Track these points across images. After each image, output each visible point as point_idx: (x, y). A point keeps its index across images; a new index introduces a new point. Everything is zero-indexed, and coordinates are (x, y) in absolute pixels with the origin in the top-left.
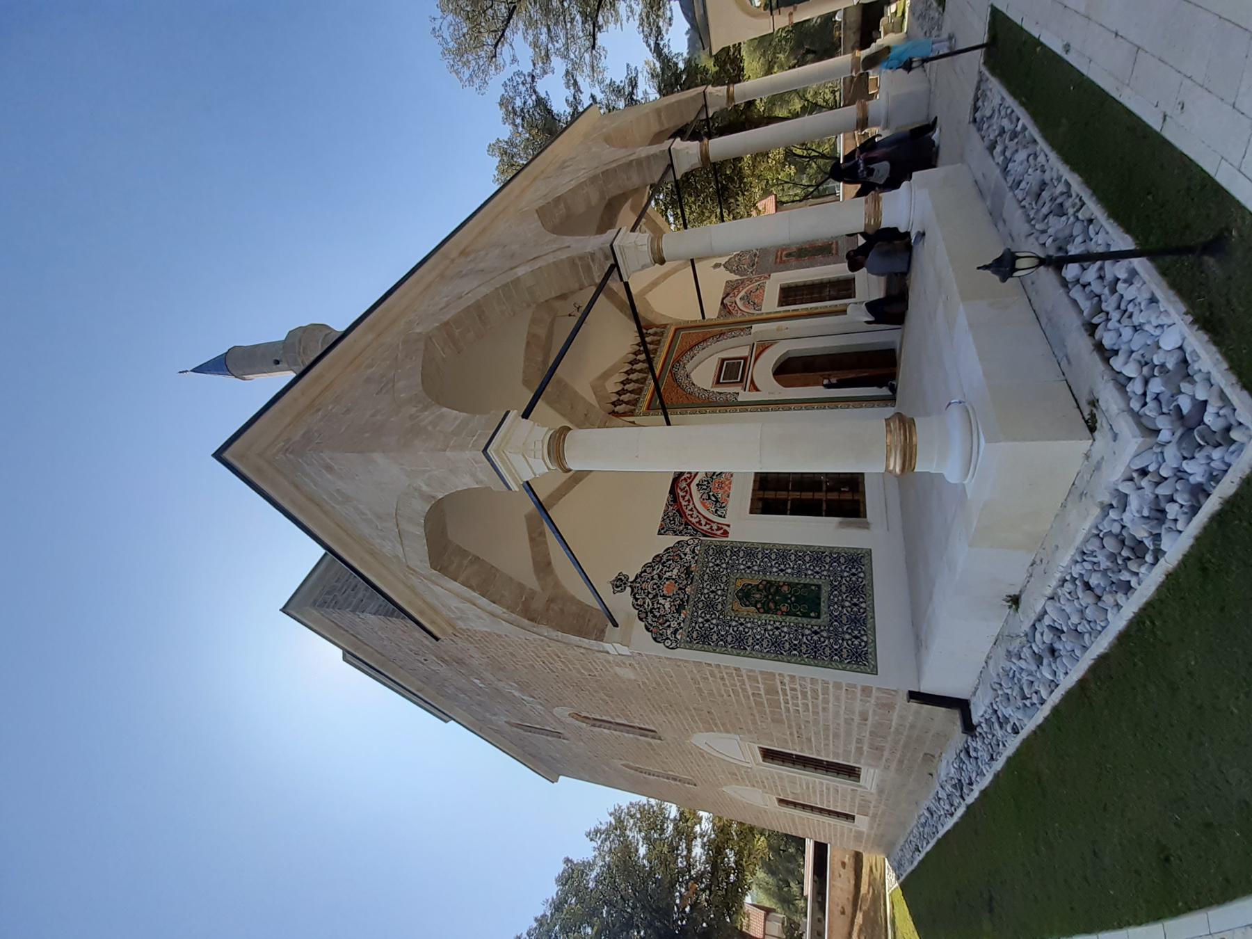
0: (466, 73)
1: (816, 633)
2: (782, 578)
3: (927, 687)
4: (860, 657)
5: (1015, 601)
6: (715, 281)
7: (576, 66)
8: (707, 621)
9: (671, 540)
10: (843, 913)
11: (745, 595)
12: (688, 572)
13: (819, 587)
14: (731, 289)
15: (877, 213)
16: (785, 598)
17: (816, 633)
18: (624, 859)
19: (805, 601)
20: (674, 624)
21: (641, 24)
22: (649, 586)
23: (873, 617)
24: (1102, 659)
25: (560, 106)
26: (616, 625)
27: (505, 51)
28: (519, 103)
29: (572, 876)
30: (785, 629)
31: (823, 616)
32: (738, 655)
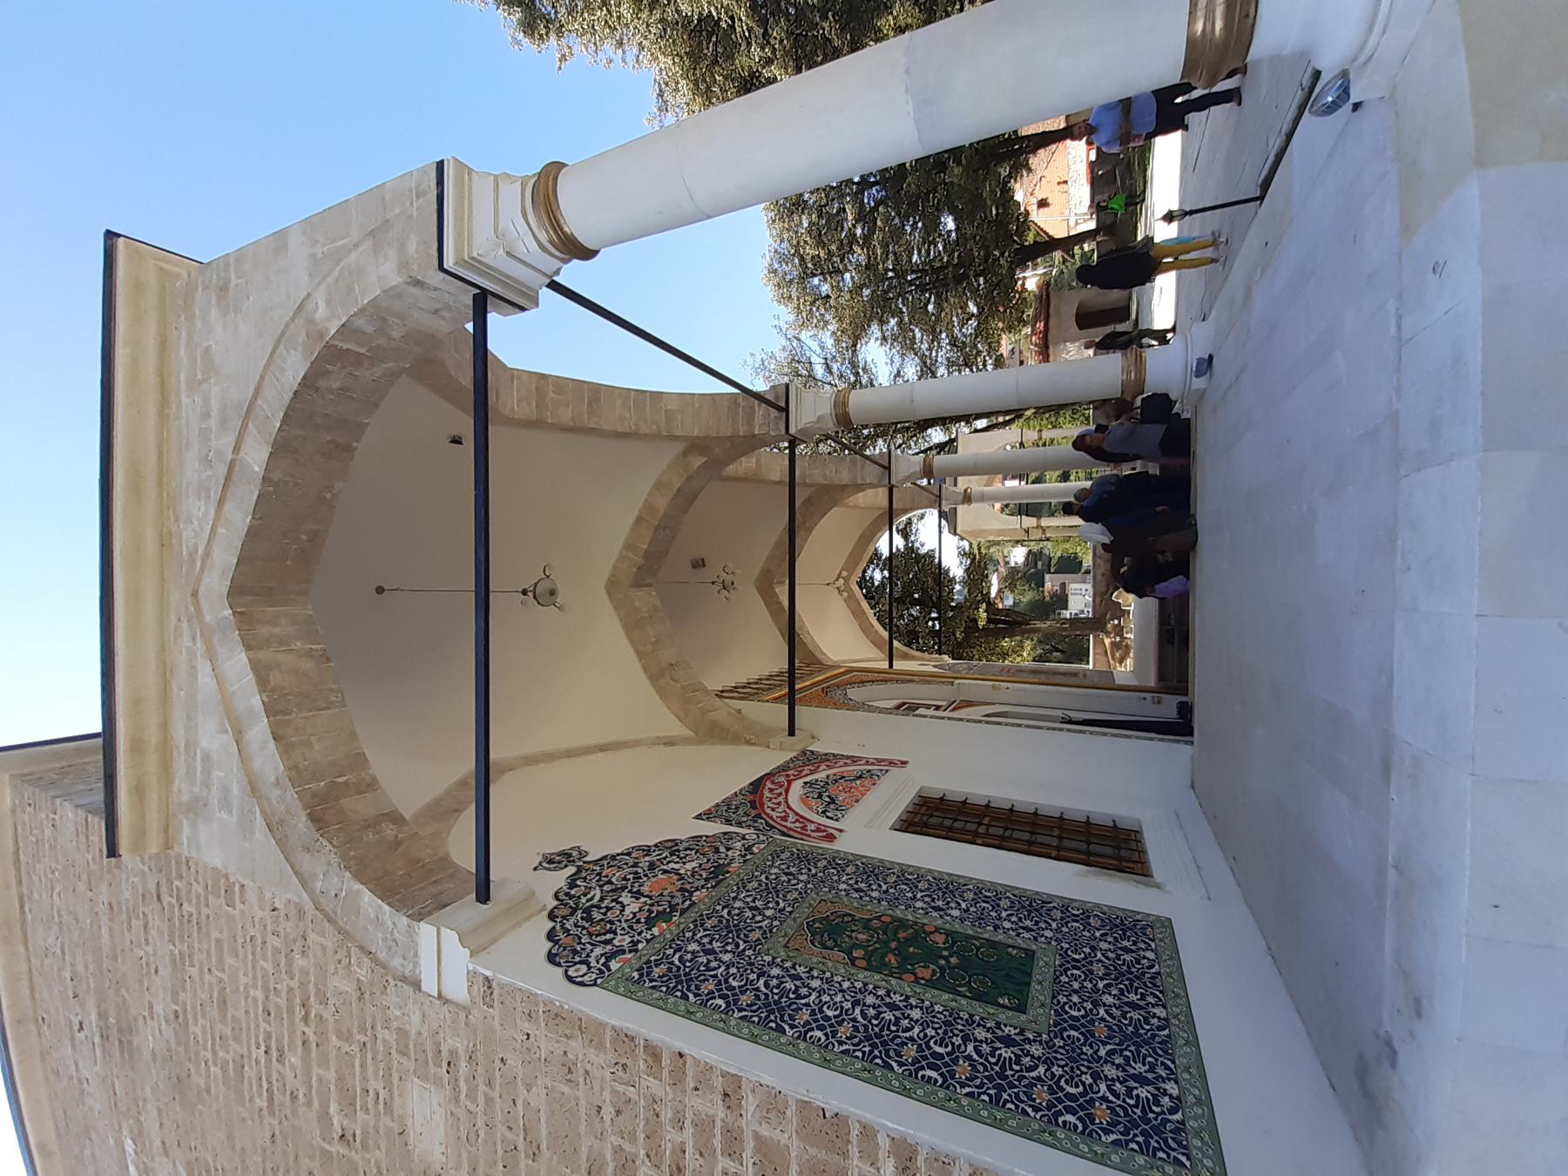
16: (932, 955)
31: (1039, 1015)
32: (753, 1039)
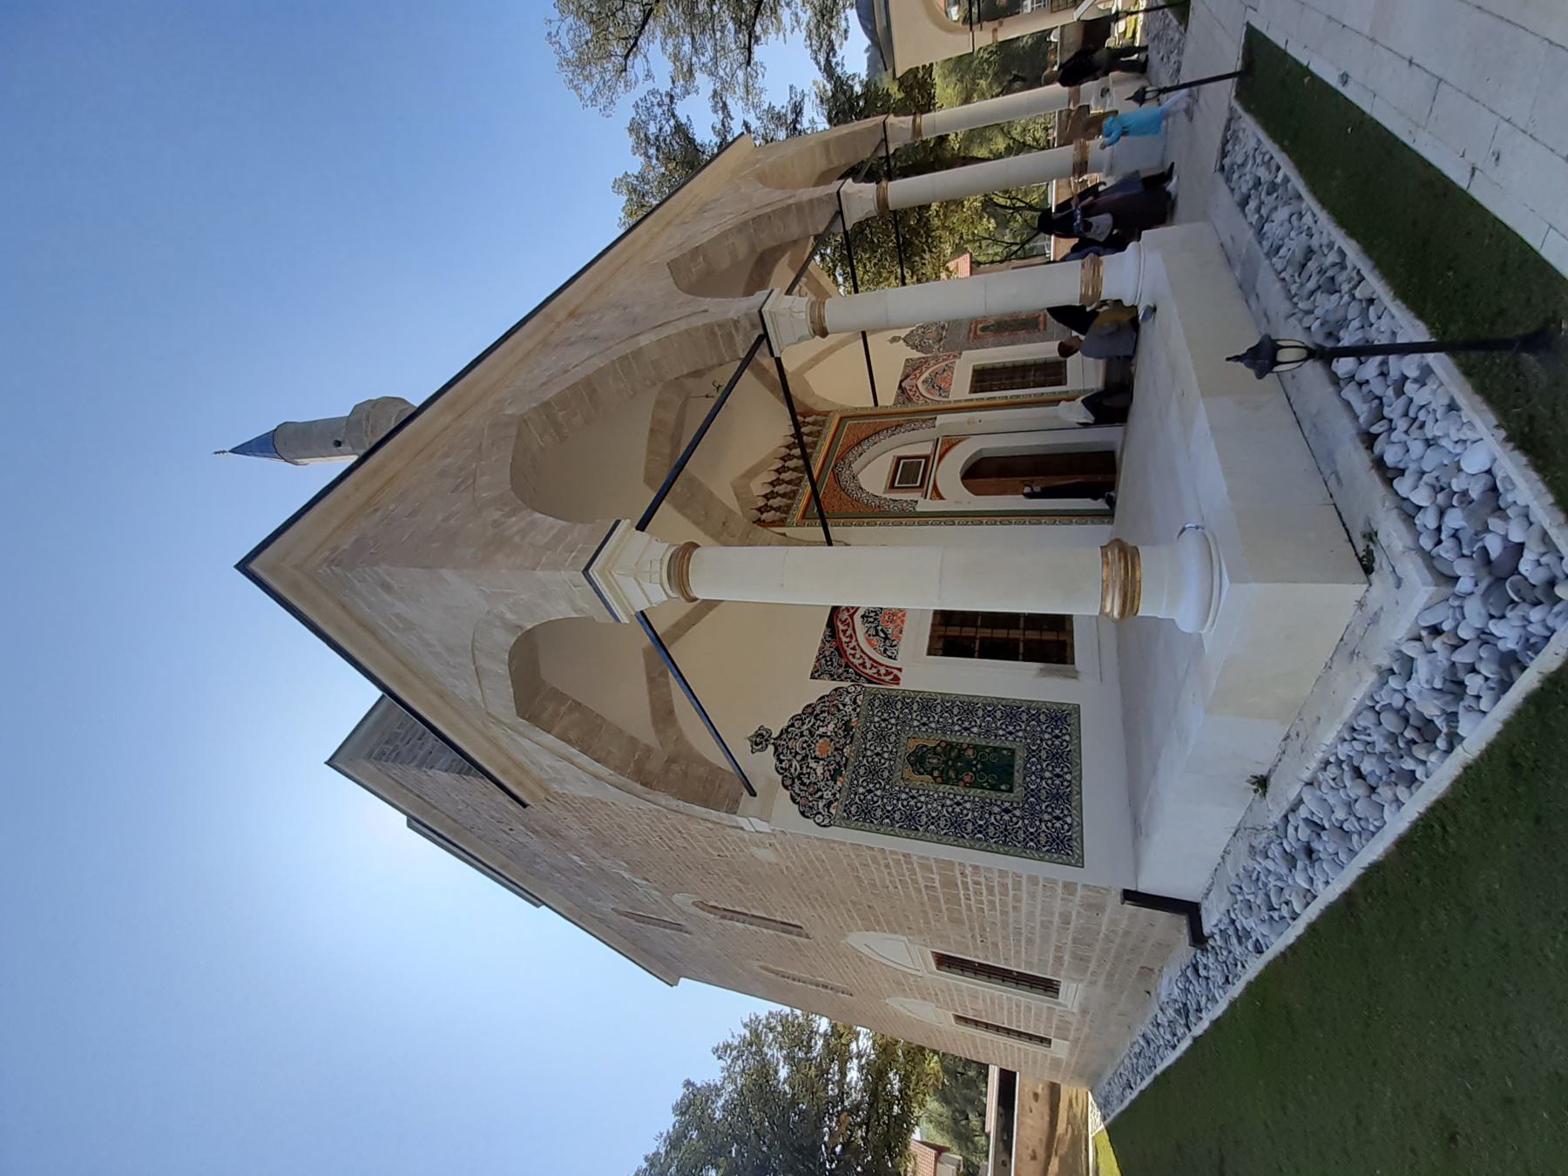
0: (588, 89)
1: (1007, 811)
2: (965, 739)
3: (1146, 886)
4: (1062, 844)
5: (1262, 783)
6: (892, 359)
7: (726, 85)
8: (870, 791)
9: (826, 686)
10: (1034, 1157)
11: (918, 760)
12: (847, 727)
13: (1013, 751)
14: (912, 369)
15: (1096, 281)
16: (969, 765)
17: (1007, 811)
18: (760, 1082)
19: (995, 770)
20: (828, 795)
21: (810, 37)
22: (797, 745)
23: (1080, 793)
24: (1374, 869)
25: (705, 135)
26: (753, 794)
27: (637, 65)
28: (653, 129)
29: (694, 1104)
30: (968, 805)
31: (1017, 790)
